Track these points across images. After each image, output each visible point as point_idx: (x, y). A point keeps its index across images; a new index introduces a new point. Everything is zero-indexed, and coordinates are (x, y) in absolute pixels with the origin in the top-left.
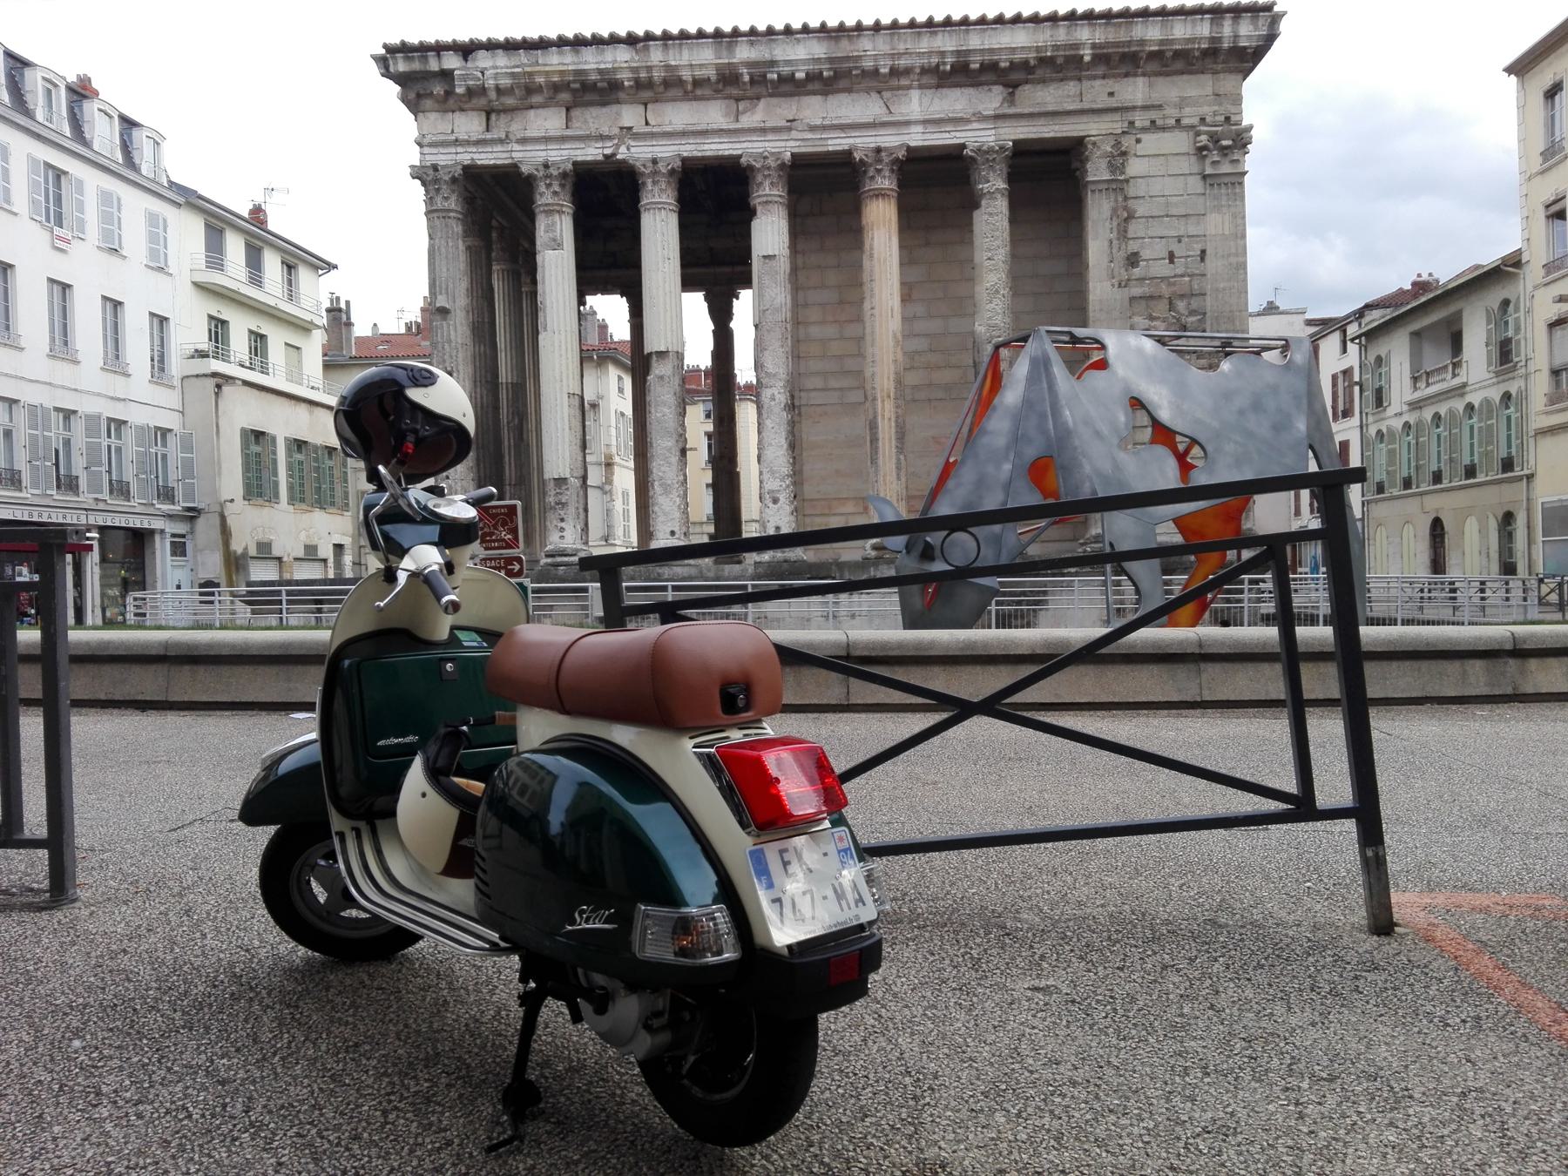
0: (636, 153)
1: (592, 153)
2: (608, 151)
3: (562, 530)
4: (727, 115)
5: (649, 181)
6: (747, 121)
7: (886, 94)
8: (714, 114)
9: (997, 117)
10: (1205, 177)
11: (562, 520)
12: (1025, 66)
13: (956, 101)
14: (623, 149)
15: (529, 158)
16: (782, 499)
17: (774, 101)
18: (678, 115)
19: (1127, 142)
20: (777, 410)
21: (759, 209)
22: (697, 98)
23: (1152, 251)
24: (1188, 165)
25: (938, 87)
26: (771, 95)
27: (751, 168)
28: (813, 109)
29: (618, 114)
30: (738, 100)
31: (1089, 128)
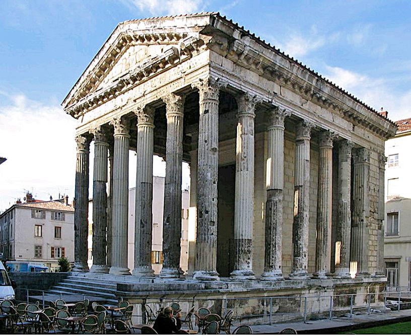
0: (282, 107)
1: (266, 98)
2: (270, 100)
3: (249, 263)
4: (300, 102)
5: (280, 118)
6: (306, 107)
7: (333, 115)
8: (296, 99)
9: (352, 133)
10: (380, 169)
11: (249, 259)
12: (360, 121)
13: (345, 124)
14: (273, 101)
15: (251, 92)
16: (307, 256)
17: (311, 103)
18: (289, 95)
19: (370, 152)
20: (307, 220)
21: (305, 141)
22: (294, 92)
23: (372, 188)
24: (377, 164)
25: (343, 118)
26: (311, 101)
27: (305, 125)
28: (319, 110)
29: (273, 86)
30: (303, 98)
31: (366, 145)
